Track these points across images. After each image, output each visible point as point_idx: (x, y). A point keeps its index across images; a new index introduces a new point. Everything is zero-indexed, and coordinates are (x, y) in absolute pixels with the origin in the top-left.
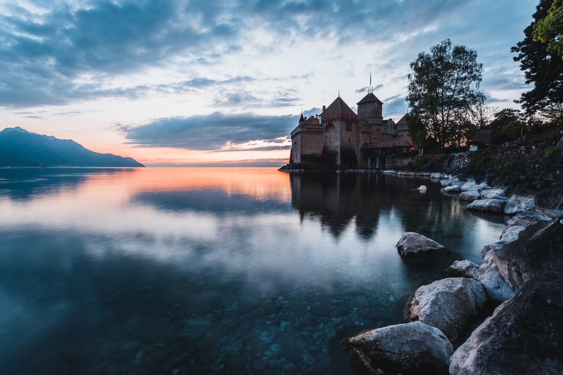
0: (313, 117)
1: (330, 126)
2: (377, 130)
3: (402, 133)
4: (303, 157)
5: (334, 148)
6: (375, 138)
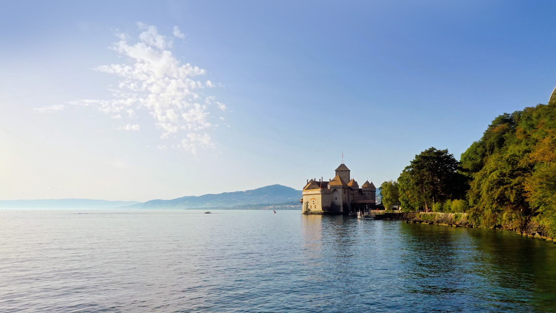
0: (312, 180)
1: (335, 190)
2: (357, 192)
3: (365, 192)
4: (323, 208)
5: (338, 203)
6: (356, 197)
